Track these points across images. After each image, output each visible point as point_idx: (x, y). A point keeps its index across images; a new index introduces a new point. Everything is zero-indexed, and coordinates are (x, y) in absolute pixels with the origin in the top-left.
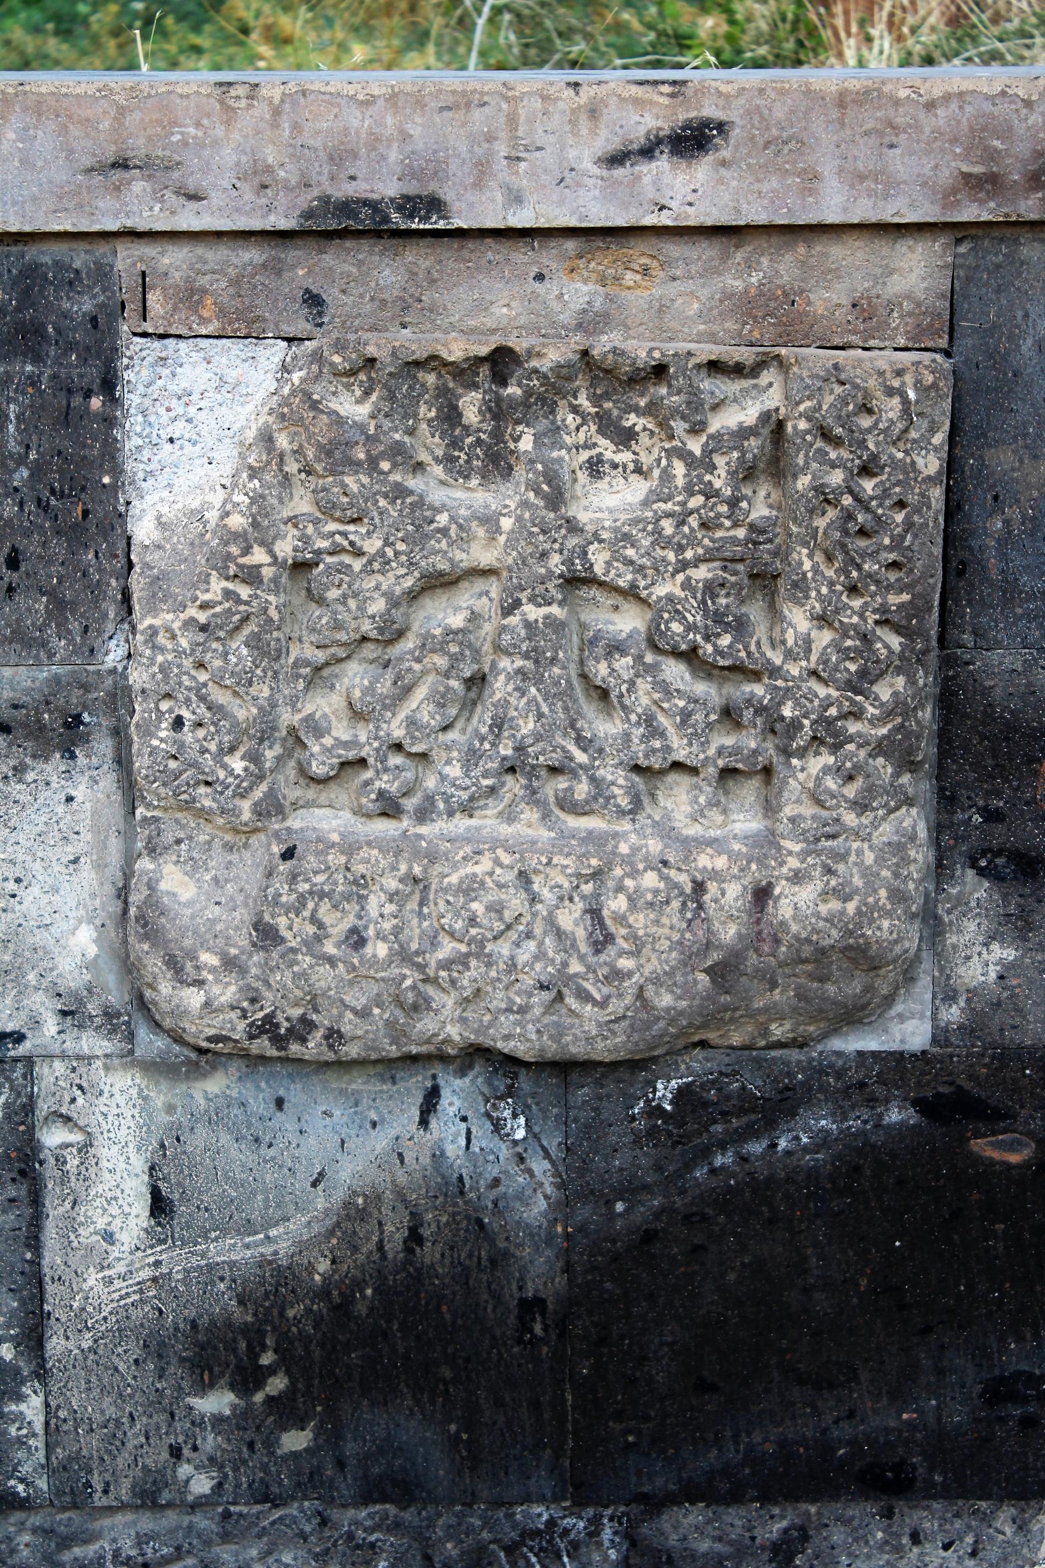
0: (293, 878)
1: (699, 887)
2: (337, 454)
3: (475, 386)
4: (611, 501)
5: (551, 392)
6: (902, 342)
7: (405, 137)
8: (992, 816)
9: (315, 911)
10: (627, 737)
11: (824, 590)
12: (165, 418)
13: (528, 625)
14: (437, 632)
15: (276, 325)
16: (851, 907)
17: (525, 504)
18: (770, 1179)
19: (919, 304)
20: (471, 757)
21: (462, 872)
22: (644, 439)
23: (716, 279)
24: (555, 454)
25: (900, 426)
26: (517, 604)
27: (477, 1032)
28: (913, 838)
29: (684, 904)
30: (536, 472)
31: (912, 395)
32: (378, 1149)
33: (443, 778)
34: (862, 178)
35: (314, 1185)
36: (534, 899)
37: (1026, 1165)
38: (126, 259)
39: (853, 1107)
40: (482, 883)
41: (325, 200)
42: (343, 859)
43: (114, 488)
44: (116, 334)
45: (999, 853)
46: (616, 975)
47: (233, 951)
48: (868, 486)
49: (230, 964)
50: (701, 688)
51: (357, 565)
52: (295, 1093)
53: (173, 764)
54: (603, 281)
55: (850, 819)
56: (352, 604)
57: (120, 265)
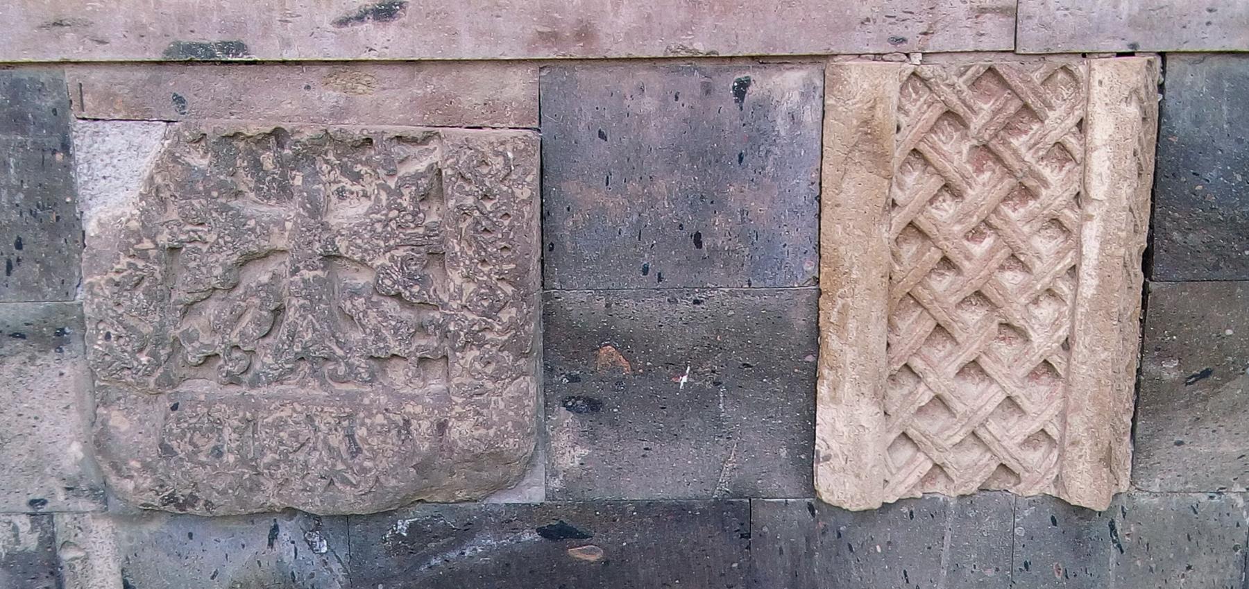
0: (178, 421)
1: (407, 422)
2: (188, 187)
3: (269, 149)
4: (351, 212)
5: (309, 154)
6: (513, 124)
7: (221, 9)
8: (574, 379)
9: (191, 438)
10: (364, 341)
11: (467, 262)
12: (100, 165)
13: (304, 281)
14: (253, 285)
15: (159, 113)
16: (492, 432)
17: (298, 215)
18: (461, 572)
19: (521, 104)
20: (278, 353)
21: (275, 416)
22: (367, 178)
23: (408, 89)
24: (315, 187)
25: (504, 173)
26: (297, 269)
27: (288, 501)
28: (527, 393)
29: (399, 432)
30: (303, 198)
31: (510, 155)
32: (247, 558)
33: (263, 364)
34: (482, 34)
35: (213, 578)
36: (316, 430)
37: (599, 561)
38: (70, 76)
39: (505, 533)
40: (286, 422)
41: (178, 44)
42: (206, 410)
43: (73, 204)
44: (68, 119)
45: (579, 398)
46: (364, 470)
47: (149, 460)
48: (488, 205)
49: (146, 467)
50: (406, 314)
51: (205, 248)
52: (198, 531)
53: (108, 358)
54: (345, 90)
55: (489, 385)
56: (204, 270)
57: (67, 80)
